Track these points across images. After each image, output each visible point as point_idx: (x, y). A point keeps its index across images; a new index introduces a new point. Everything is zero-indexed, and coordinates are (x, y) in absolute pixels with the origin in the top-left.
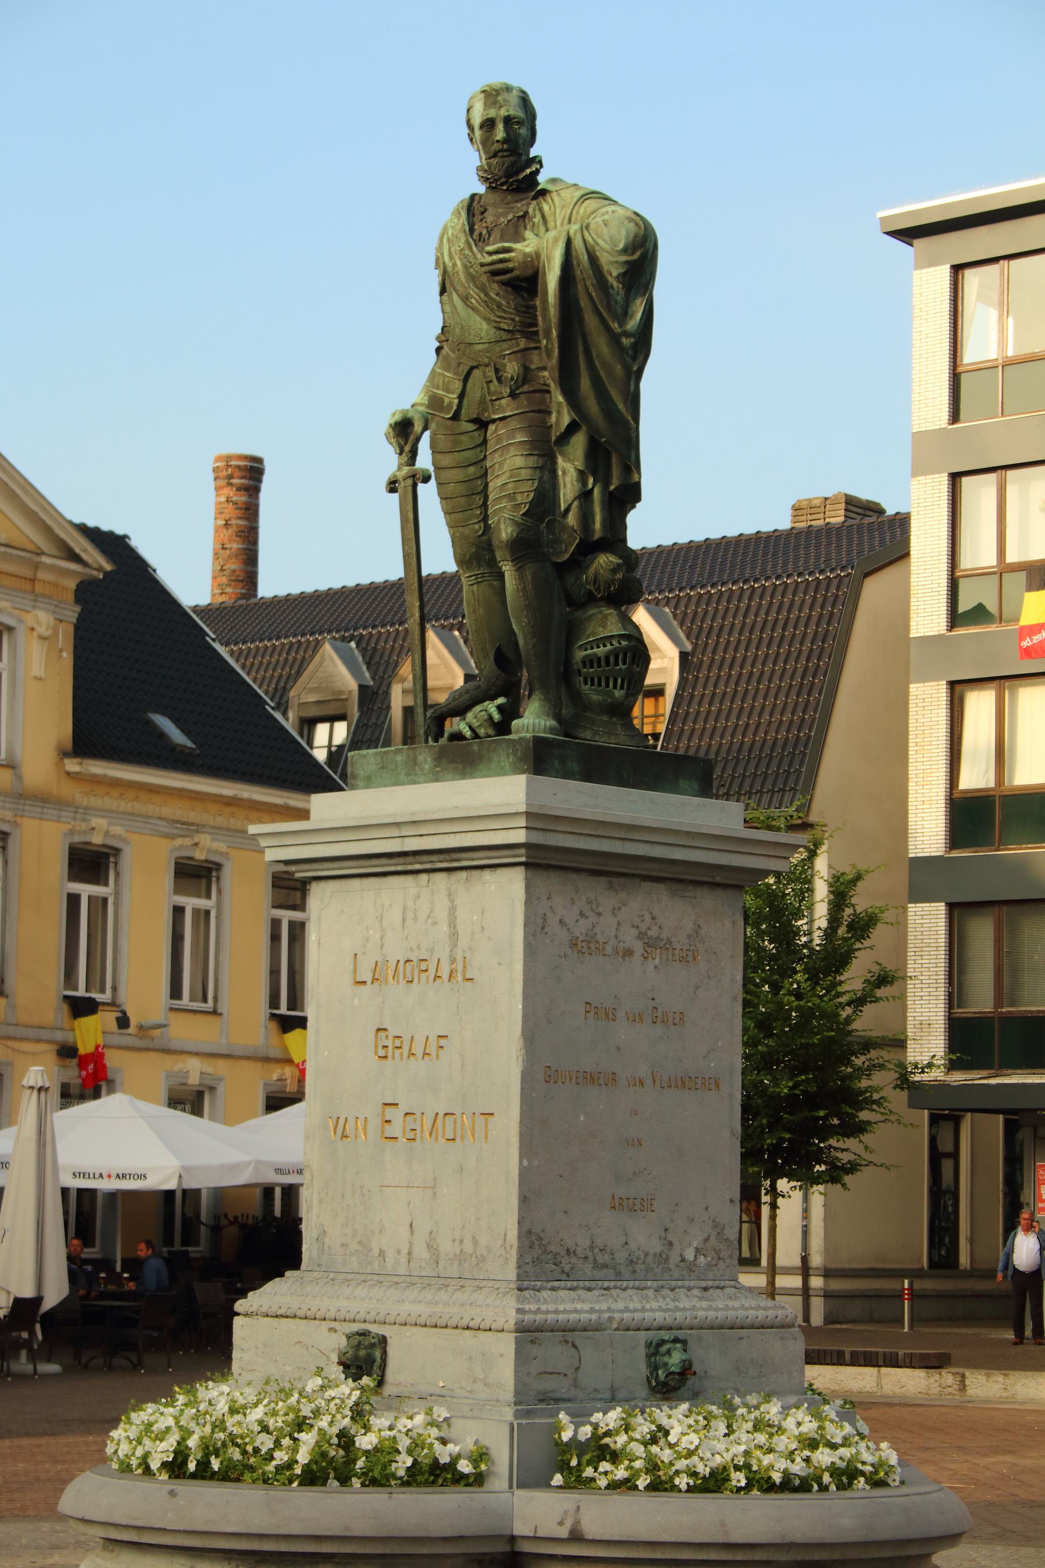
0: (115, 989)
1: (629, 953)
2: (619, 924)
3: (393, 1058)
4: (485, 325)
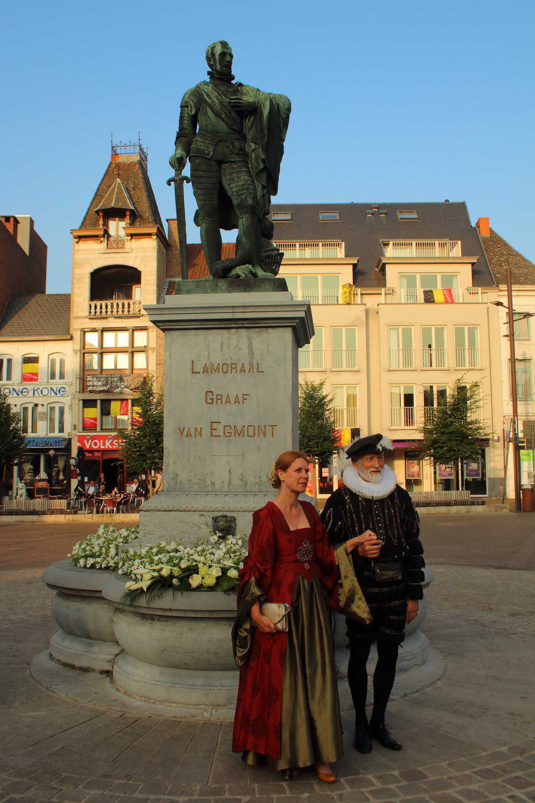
3: (217, 403)
4: (225, 126)
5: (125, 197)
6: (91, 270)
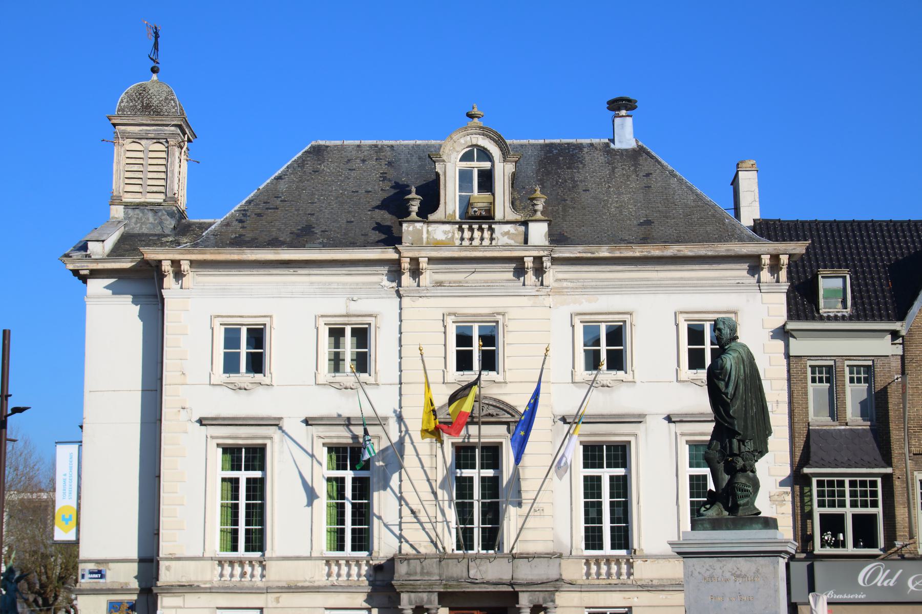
1: (727, 580)
2: (723, 572)
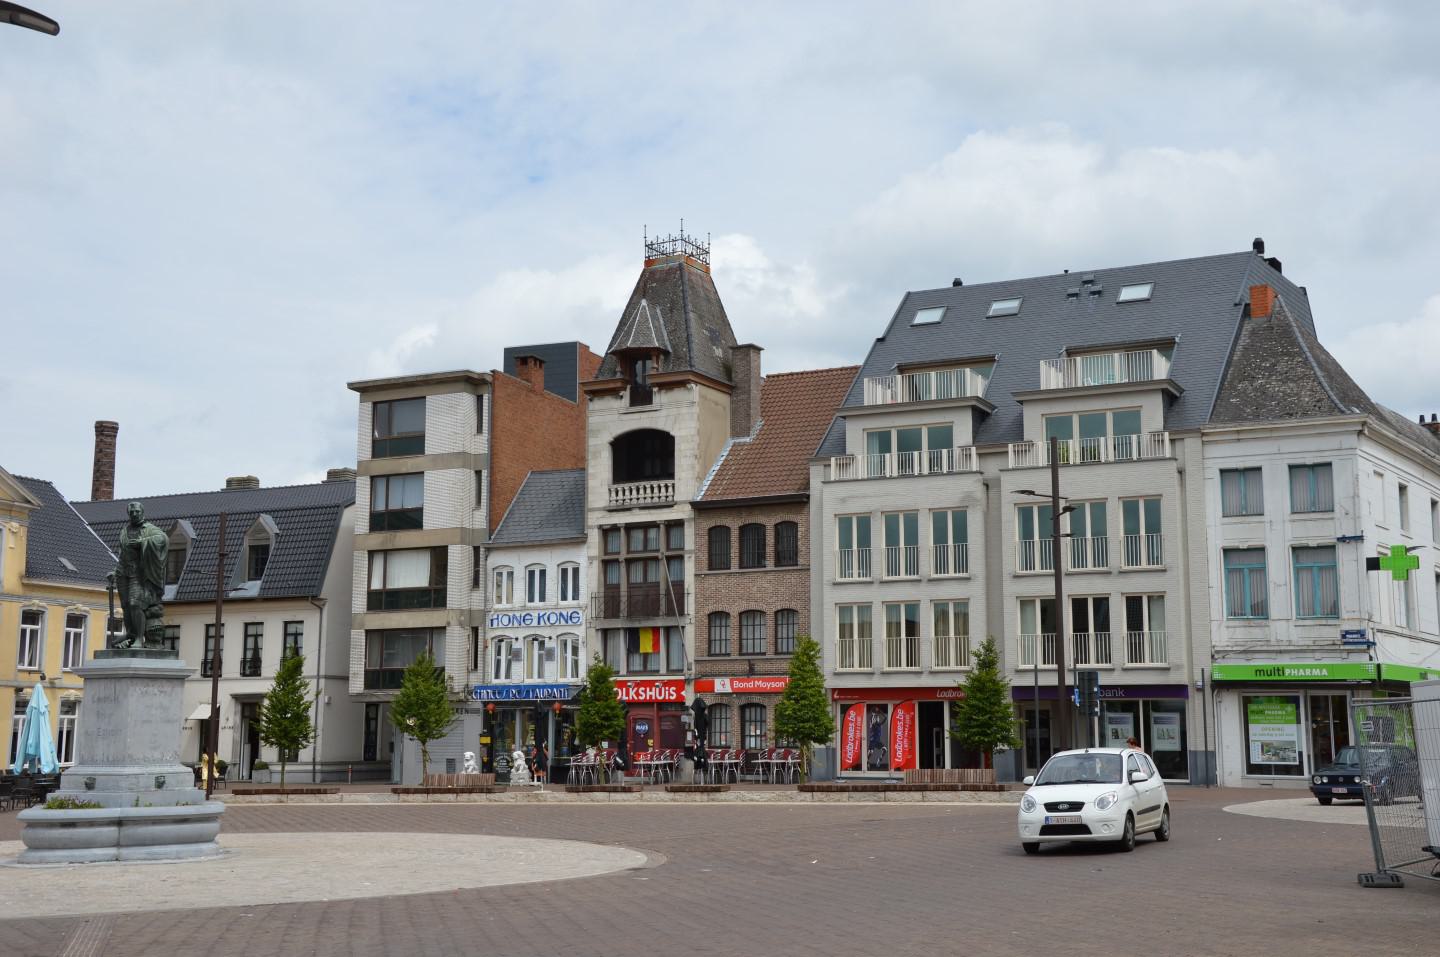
0: (40, 665)
5: (649, 328)
6: (611, 438)
